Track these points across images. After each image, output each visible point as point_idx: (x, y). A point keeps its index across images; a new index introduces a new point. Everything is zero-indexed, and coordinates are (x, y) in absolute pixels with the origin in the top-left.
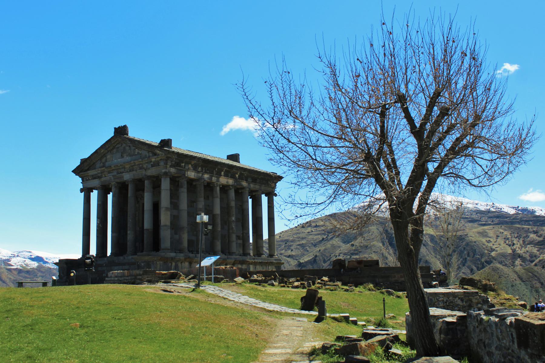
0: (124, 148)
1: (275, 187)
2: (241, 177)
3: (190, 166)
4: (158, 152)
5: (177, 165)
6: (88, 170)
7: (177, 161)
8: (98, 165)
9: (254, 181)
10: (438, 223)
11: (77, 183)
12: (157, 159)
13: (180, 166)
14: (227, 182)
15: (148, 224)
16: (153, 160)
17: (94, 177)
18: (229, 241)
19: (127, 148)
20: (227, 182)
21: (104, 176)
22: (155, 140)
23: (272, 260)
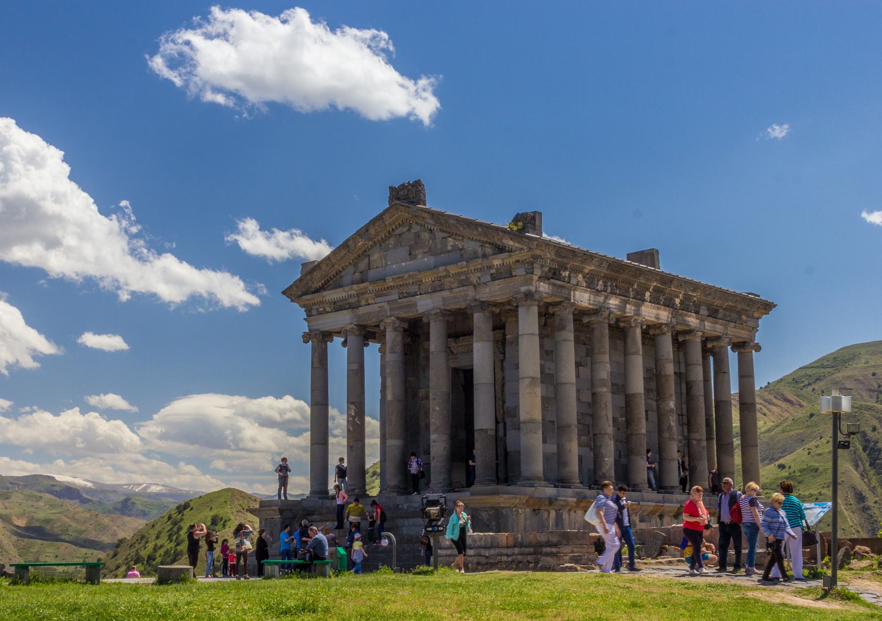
0: (417, 235)
1: (755, 329)
4: (511, 243)
5: (553, 275)
6: (322, 288)
8: (347, 278)
9: (713, 313)
12: (507, 261)
16: (497, 262)
17: (338, 307)
19: (425, 235)
21: (363, 302)
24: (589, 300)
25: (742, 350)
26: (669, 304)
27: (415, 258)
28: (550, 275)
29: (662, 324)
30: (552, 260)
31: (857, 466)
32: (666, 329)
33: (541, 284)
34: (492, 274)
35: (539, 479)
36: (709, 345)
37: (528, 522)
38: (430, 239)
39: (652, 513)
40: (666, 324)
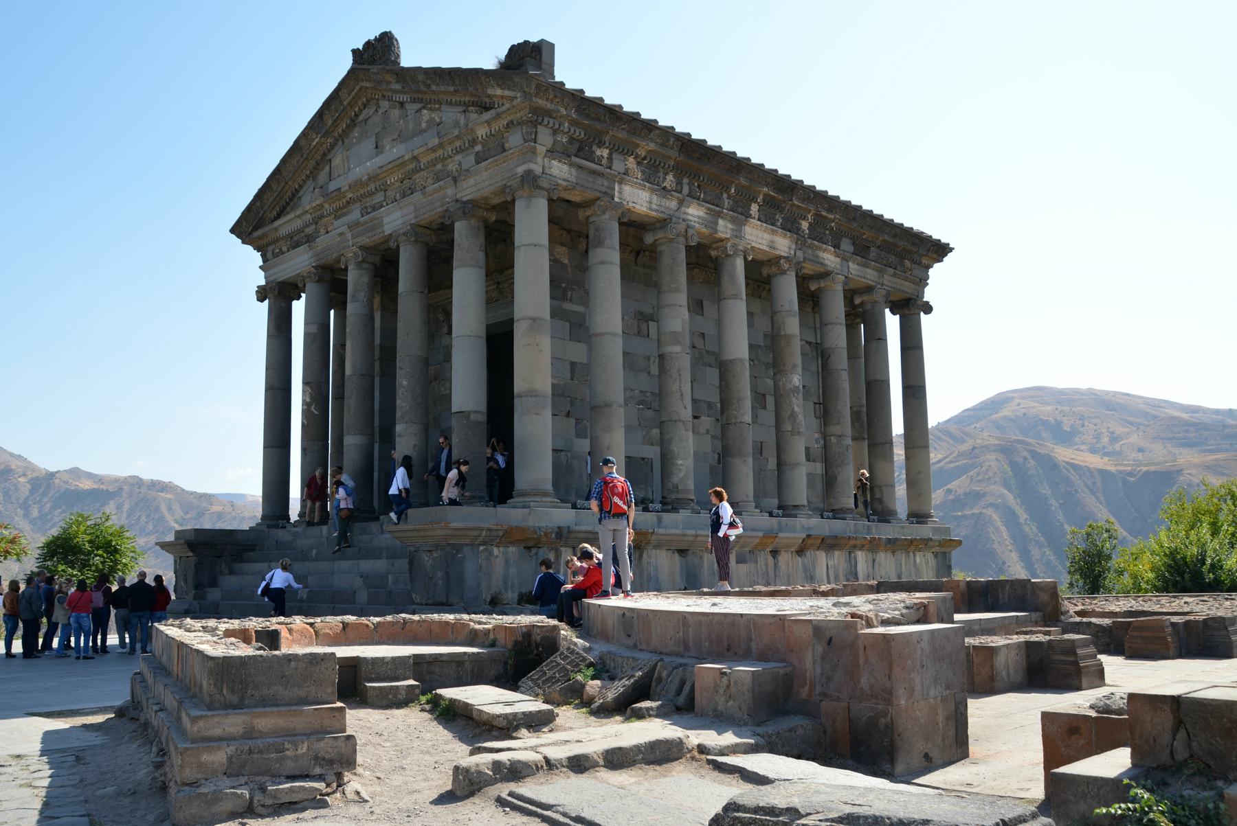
1: (923, 282)
2: (821, 233)
4: (499, 92)
5: (579, 150)
7: (579, 134)
9: (861, 250)
10: (1117, 447)
11: (248, 267)
12: (496, 126)
14: (772, 245)
15: (466, 390)
16: (482, 132)
18: (780, 464)
19: (396, 113)
20: (772, 245)
22: (487, 55)
23: (924, 531)
24: (650, 203)
25: (907, 312)
26: (790, 226)
27: (382, 152)
29: (780, 257)
31: (1010, 490)
32: (786, 266)
33: (555, 163)
36: (857, 301)
37: (513, 570)
38: (400, 117)
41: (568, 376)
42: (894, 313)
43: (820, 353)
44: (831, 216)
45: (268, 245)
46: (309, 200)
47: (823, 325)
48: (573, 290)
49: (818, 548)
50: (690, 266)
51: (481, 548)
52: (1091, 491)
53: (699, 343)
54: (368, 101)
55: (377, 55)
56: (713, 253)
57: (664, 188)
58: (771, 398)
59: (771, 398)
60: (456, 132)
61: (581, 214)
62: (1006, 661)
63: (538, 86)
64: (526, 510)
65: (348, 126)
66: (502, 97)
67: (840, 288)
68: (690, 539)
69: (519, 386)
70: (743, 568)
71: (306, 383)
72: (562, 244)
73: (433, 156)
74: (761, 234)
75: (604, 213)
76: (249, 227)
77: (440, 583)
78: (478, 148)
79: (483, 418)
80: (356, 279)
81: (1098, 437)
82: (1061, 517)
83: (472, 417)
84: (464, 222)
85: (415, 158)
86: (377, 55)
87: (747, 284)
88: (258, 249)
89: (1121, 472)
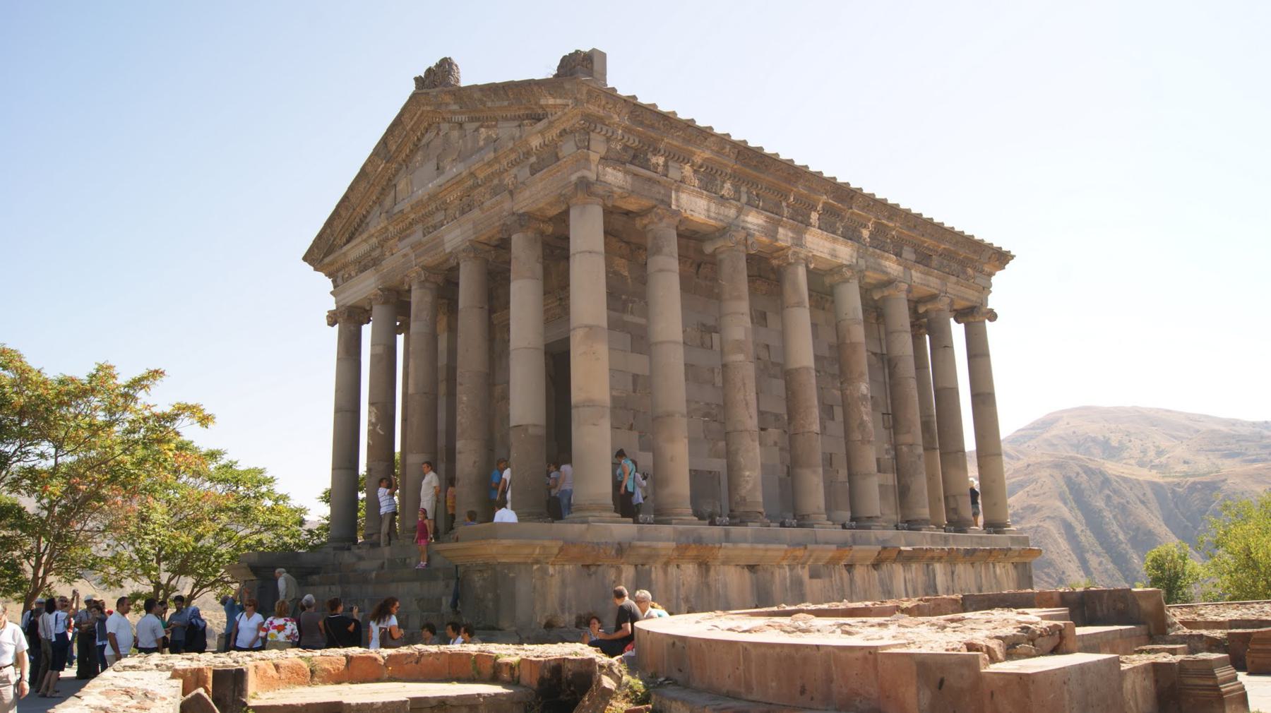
1: (986, 289)
3: (687, 169)
4: (551, 101)
7: (633, 142)
9: (924, 259)
10: (1163, 459)
11: (320, 292)
13: (645, 165)
15: (525, 403)
16: (535, 142)
17: (364, 265)
18: (851, 475)
19: (455, 134)
23: (1000, 541)
24: (708, 210)
25: (971, 320)
26: (851, 235)
28: (627, 157)
29: (842, 266)
30: (627, 130)
31: (1066, 504)
32: (848, 274)
33: (609, 170)
34: (531, 166)
35: (604, 508)
36: (921, 310)
37: (570, 591)
39: (833, 562)
40: (849, 266)
41: (630, 388)
42: (957, 321)
43: (886, 363)
44: (891, 224)
45: (338, 271)
46: (377, 223)
47: (888, 333)
48: (633, 302)
49: (895, 561)
50: (752, 278)
51: (535, 567)
52: (1143, 502)
53: (764, 354)
54: (430, 125)
55: (438, 79)
56: (775, 262)
57: (722, 197)
58: (838, 408)
59: (838, 408)
60: (511, 145)
61: (639, 223)
62: (1133, 688)
63: (589, 93)
64: (584, 526)
65: (411, 151)
66: (555, 106)
67: (903, 295)
68: (761, 553)
69: (576, 396)
70: (817, 584)
71: (371, 404)
72: (622, 257)
73: (490, 171)
74: (822, 242)
75: (661, 220)
76: (321, 254)
77: (491, 605)
78: (533, 159)
79: (542, 432)
80: (419, 298)
81: (1144, 452)
82: (1115, 527)
83: (531, 430)
84: (521, 235)
85: (472, 174)
86: (438, 79)
87: (810, 296)
88: (329, 275)
89: (1169, 484)
